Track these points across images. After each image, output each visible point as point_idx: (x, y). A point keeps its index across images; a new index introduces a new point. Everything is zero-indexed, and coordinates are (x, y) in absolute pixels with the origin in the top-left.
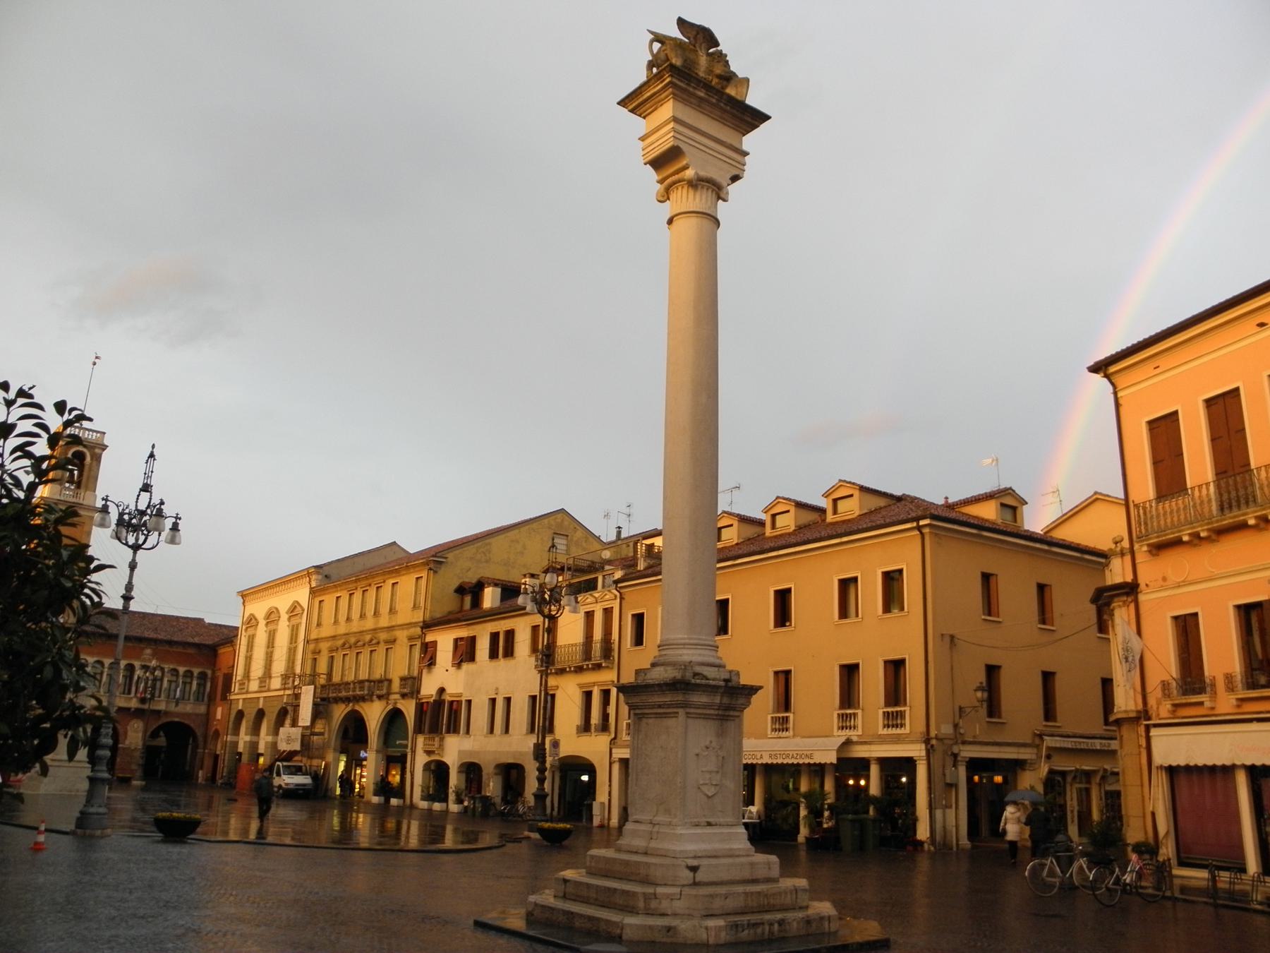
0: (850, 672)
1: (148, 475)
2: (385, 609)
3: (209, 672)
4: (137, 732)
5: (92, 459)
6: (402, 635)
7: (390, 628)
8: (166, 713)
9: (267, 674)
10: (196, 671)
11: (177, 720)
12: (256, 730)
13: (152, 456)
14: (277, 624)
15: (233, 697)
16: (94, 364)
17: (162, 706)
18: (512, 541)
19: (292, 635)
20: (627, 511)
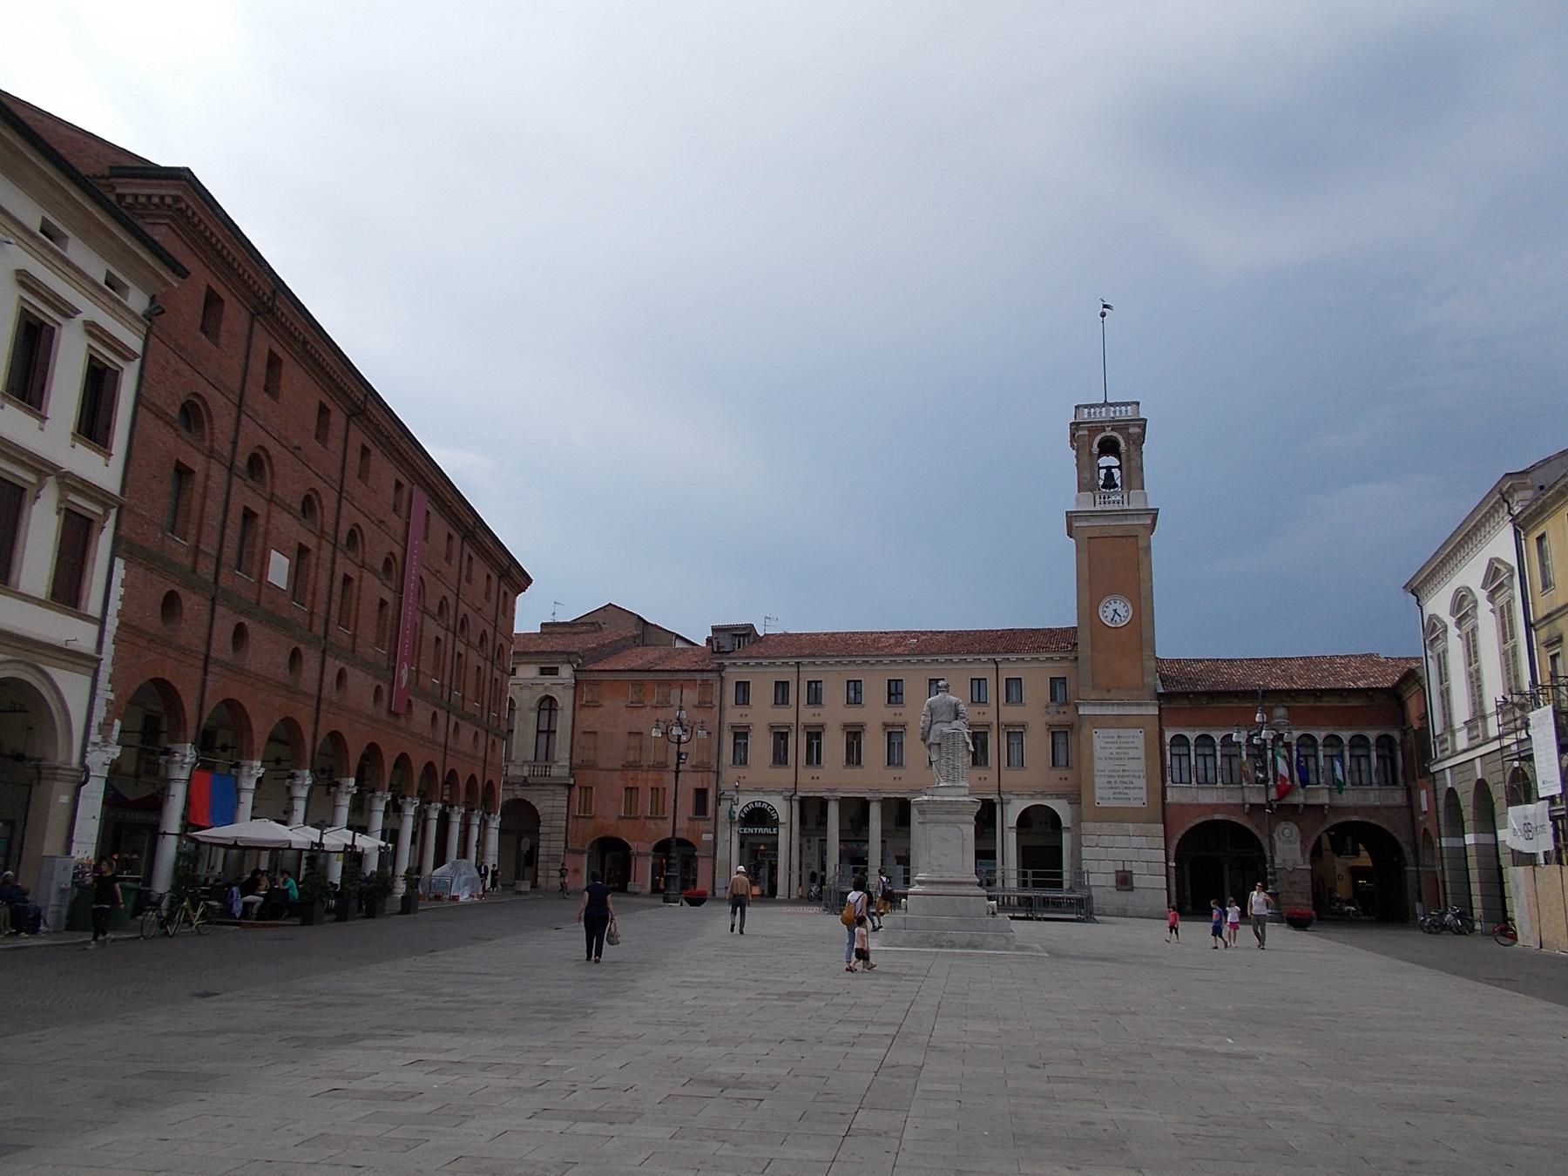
3: (1396, 735)
9: (1479, 716)
10: (1372, 735)
11: (1355, 818)
14: (1476, 617)
16: (1103, 315)
17: (1323, 798)
19: (1503, 625)
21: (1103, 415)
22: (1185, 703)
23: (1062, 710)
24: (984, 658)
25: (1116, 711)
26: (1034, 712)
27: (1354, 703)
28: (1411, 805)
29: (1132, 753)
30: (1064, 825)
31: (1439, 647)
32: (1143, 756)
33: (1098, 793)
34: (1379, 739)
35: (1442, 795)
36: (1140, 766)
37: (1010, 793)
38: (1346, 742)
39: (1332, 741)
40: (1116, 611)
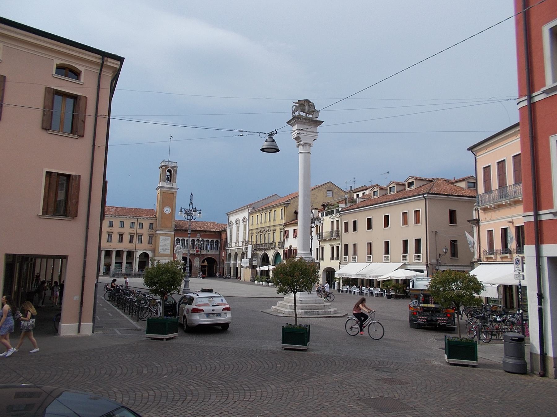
0: (405, 242)
1: (191, 200)
2: (272, 219)
4: (197, 261)
5: (174, 172)
6: (278, 228)
7: (274, 226)
8: (206, 255)
9: (237, 242)
10: (215, 240)
11: (210, 257)
12: (235, 259)
13: (191, 195)
14: (239, 224)
15: (227, 249)
17: (205, 253)
18: (313, 194)
20: (354, 180)
21: (169, 164)
22: (180, 232)
23: (152, 231)
24: (135, 217)
25: (165, 232)
26: (145, 231)
27: (213, 234)
28: (220, 255)
29: (168, 242)
30: (150, 257)
31: (231, 227)
32: (170, 242)
33: (160, 250)
34: (216, 241)
35: (228, 254)
36: (169, 245)
37: (138, 249)
38: (210, 241)
39: (208, 241)
40: (167, 210)
